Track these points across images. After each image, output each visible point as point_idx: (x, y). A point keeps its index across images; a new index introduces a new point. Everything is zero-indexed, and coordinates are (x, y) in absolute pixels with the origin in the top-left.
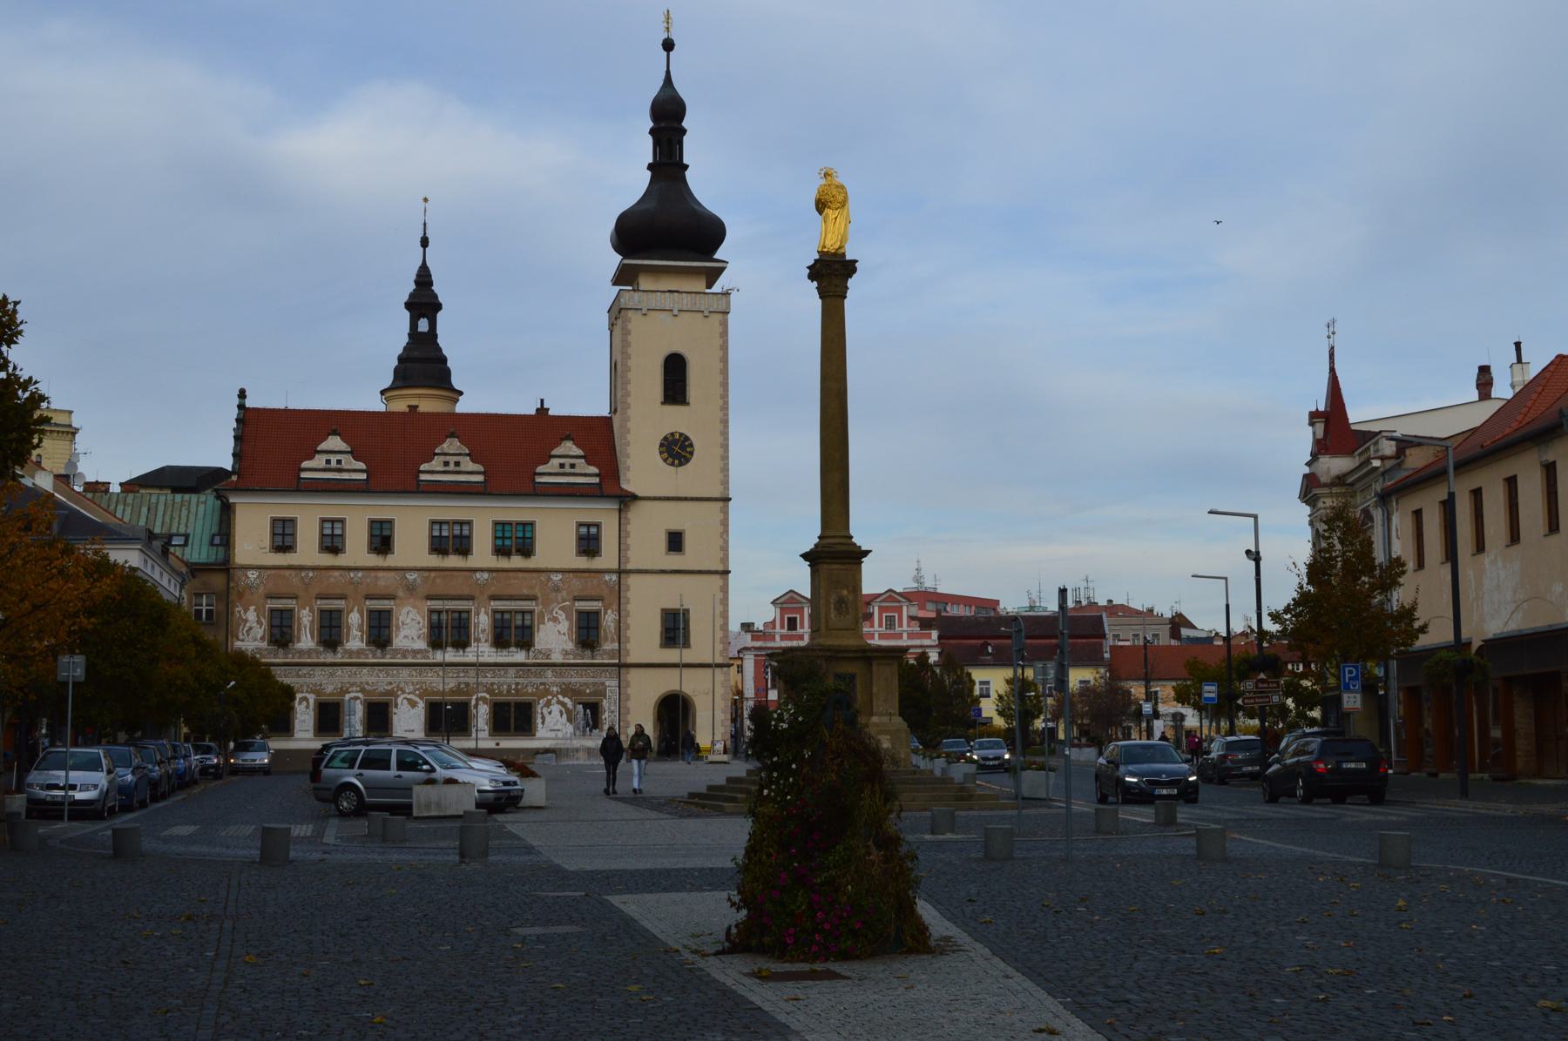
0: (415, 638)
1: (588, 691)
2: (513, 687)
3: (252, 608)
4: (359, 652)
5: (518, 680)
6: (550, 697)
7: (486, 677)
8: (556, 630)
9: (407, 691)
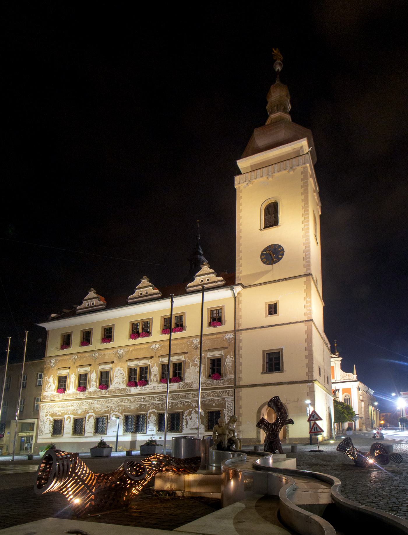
0: (121, 383)
1: (214, 405)
3: (52, 376)
4: (95, 392)
5: (173, 401)
6: (191, 410)
7: (155, 400)
8: (196, 371)
9: (115, 411)
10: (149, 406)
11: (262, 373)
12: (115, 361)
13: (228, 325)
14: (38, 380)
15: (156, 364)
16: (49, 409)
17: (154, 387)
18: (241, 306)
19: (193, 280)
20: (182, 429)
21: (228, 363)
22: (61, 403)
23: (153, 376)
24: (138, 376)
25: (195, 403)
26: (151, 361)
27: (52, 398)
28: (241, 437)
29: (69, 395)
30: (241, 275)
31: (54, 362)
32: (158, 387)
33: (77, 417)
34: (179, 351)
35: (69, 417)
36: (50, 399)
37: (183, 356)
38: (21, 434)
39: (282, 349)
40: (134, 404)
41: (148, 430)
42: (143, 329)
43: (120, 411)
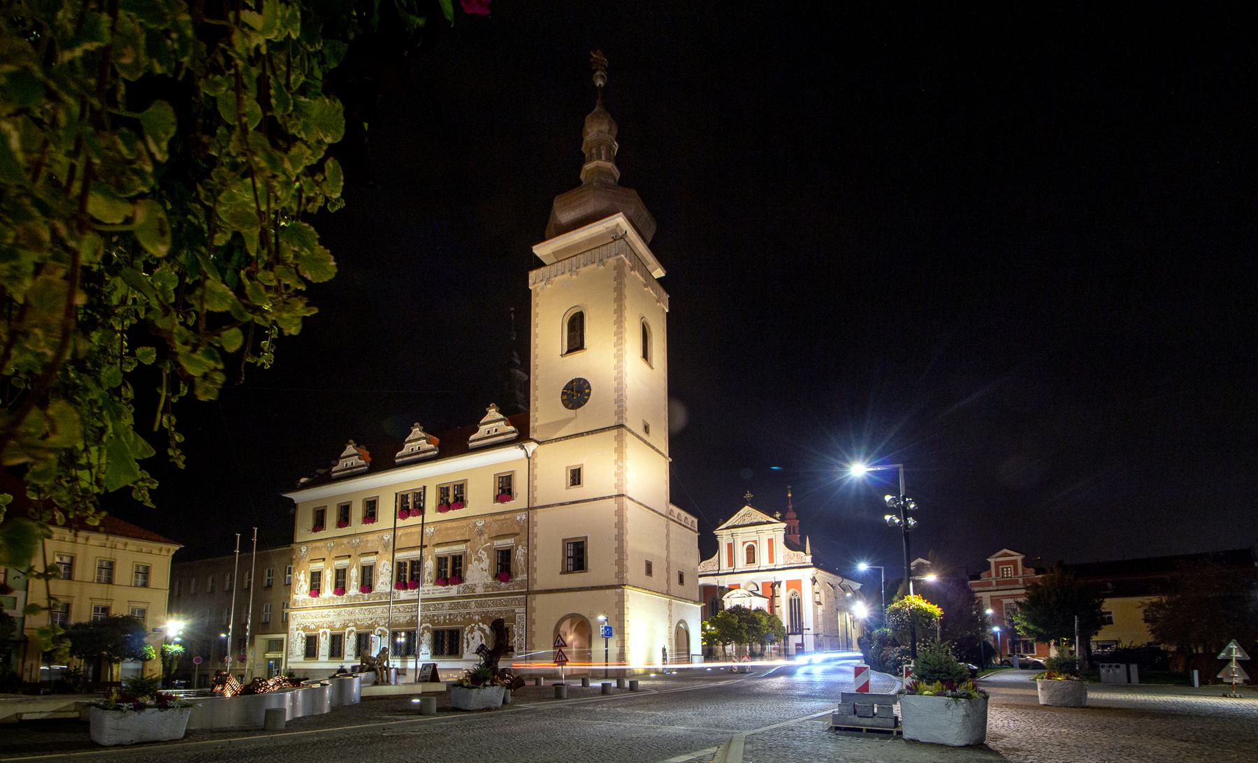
2: (448, 617)
3: (303, 571)
4: (356, 597)
5: (451, 612)
6: (473, 625)
11: (561, 573)
12: (380, 551)
13: (519, 501)
14: (288, 576)
16: (299, 620)
17: (428, 591)
18: (537, 471)
19: (476, 430)
20: (463, 653)
21: (519, 558)
22: (314, 611)
23: (426, 574)
24: (408, 574)
27: (304, 604)
29: (324, 600)
30: (537, 424)
32: (433, 590)
33: (335, 632)
34: (458, 538)
35: (325, 633)
38: (268, 655)
39: (586, 538)
40: (403, 614)
41: (420, 654)
42: (415, 502)
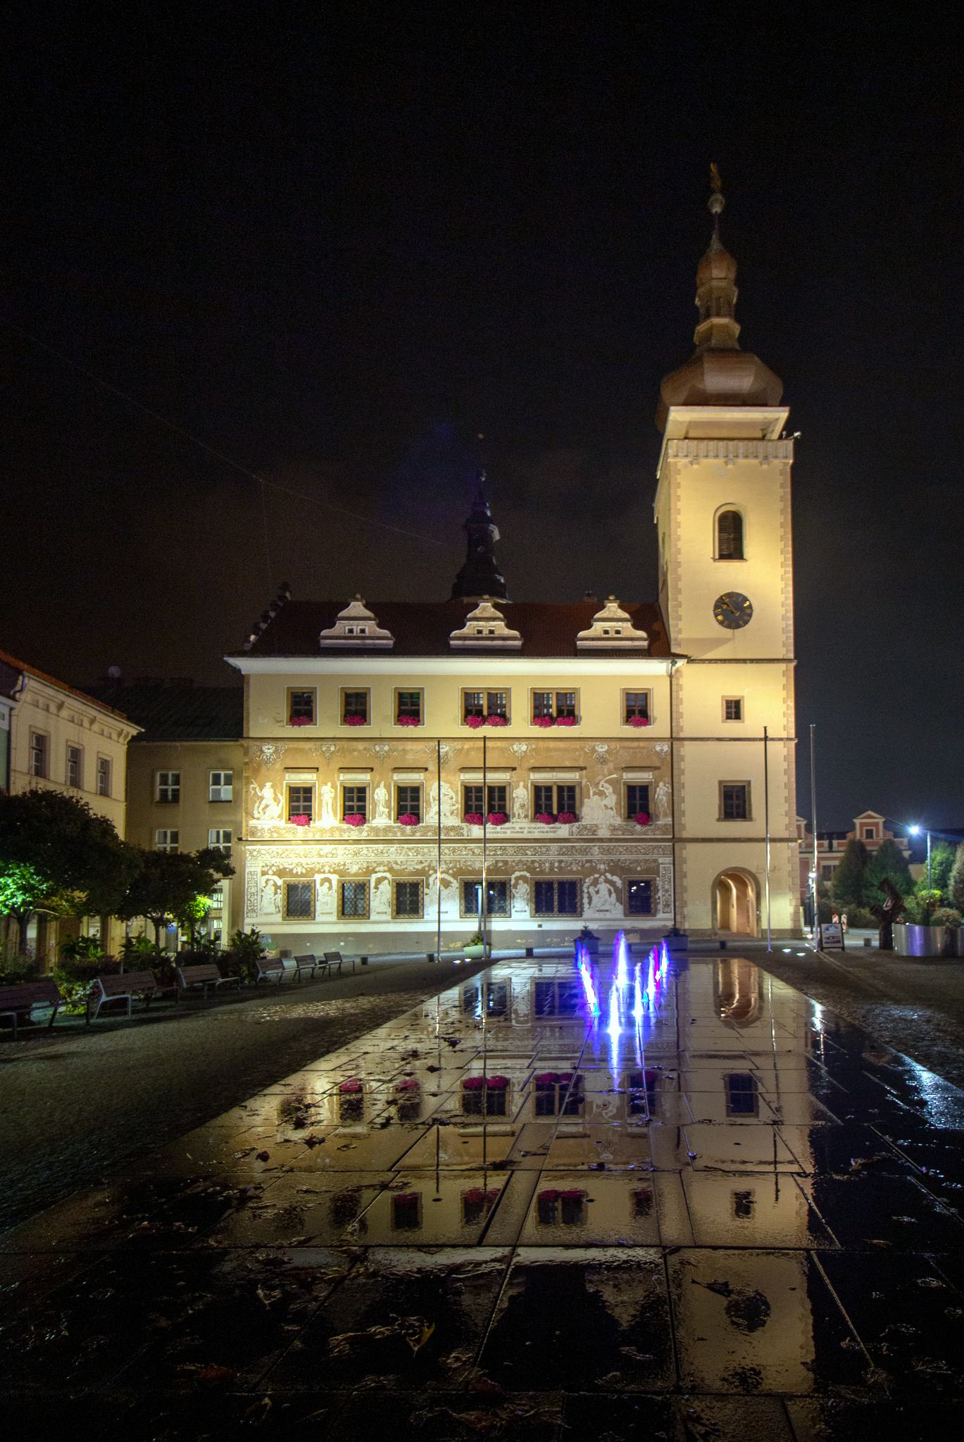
1: (639, 869)
4: (387, 829)
5: (561, 858)
6: (597, 876)
7: (527, 855)
10: (514, 864)
13: (659, 727)
15: (522, 784)
17: (521, 828)
25: (604, 863)
26: (511, 777)
28: (687, 926)
31: (271, 751)
34: (568, 764)
36: (269, 835)
37: (577, 774)
41: (513, 911)
43: (451, 871)
